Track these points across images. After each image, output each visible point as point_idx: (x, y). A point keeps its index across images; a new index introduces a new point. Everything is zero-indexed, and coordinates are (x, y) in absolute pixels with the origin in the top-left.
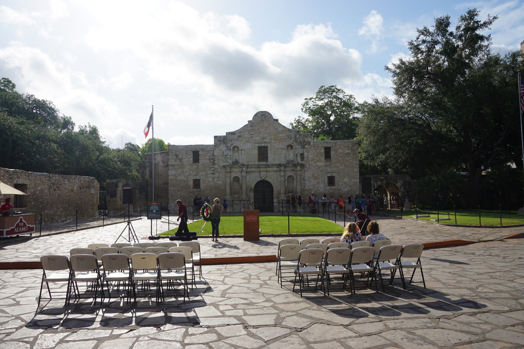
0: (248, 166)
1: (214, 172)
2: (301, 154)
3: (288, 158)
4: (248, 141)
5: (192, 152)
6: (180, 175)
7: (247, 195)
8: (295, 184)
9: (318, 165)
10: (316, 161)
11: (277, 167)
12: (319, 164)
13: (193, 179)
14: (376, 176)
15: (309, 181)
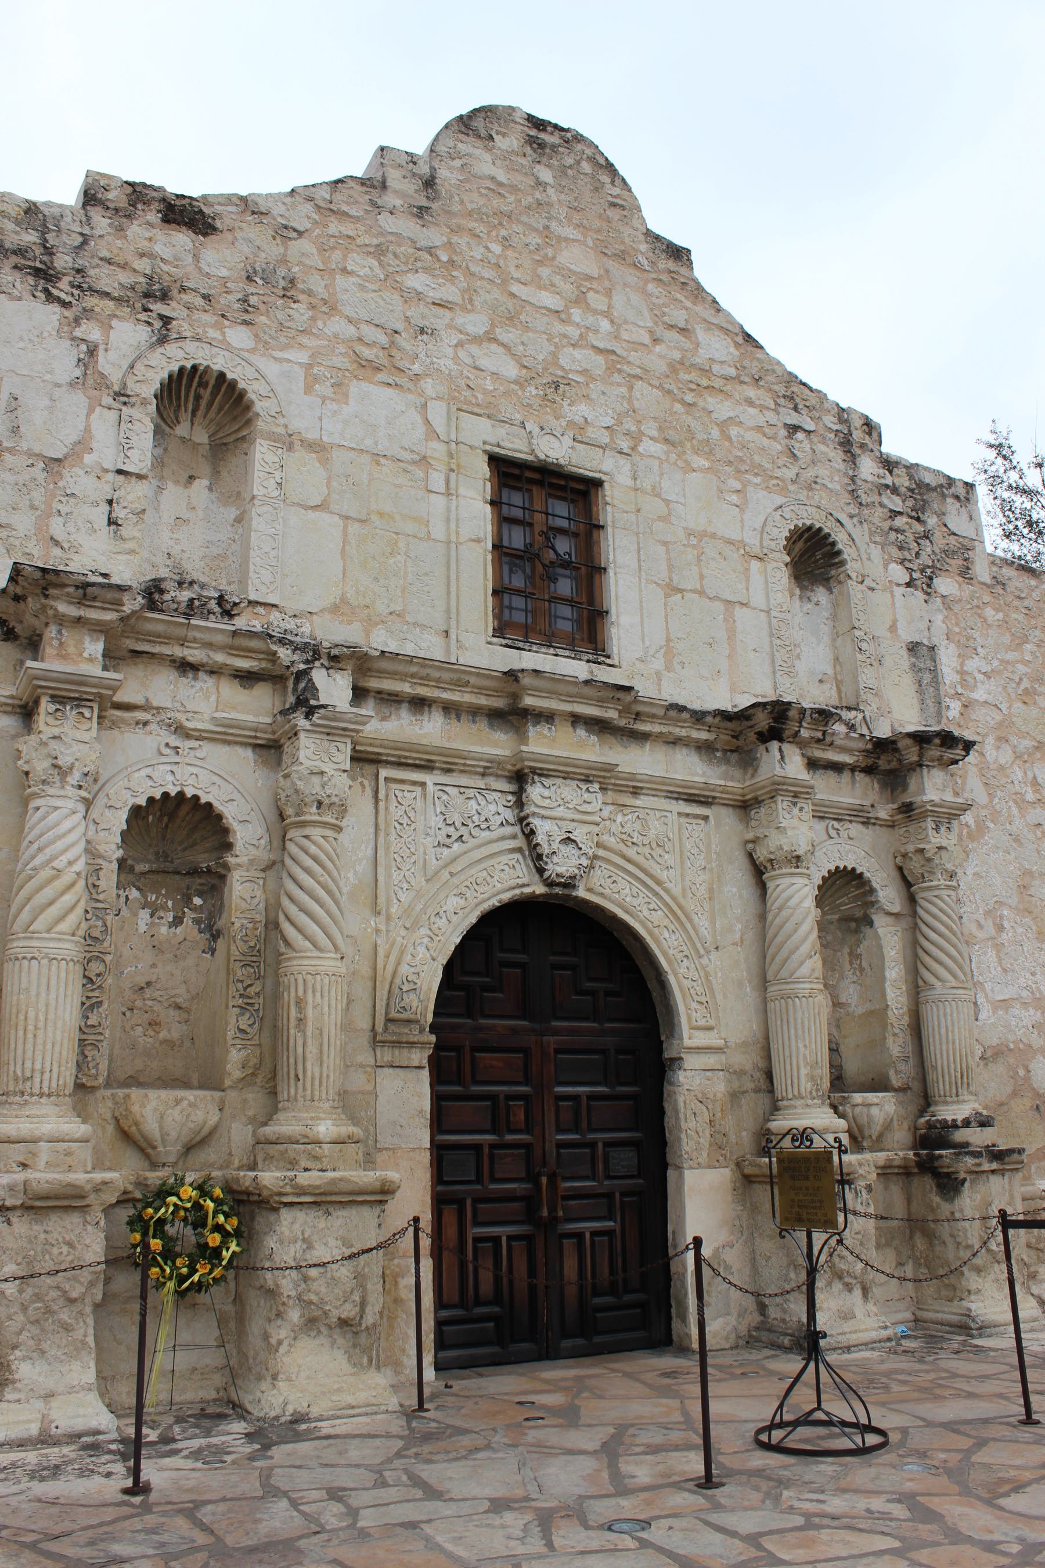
2: (913, 648)
4: (367, 353)
8: (894, 973)
11: (705, 748)
15: (999, 947)
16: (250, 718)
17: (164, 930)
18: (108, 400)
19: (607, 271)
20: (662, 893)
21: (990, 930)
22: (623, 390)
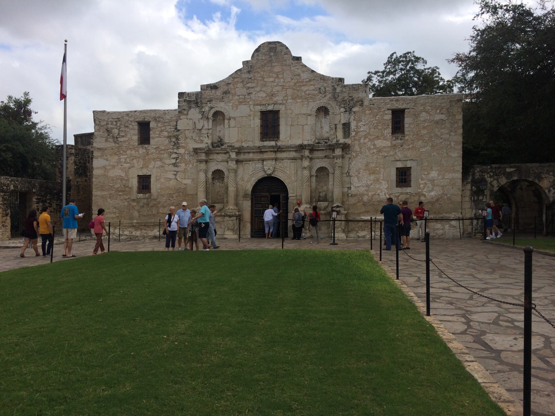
0: (240, 151)
1: (178, 161)
2: (344, 124)
3: (318, 134)
4: (241, 100)
5: (137, 123)
6: (114, 167)
7: (237, 204)
9: (377, 146)
10: (373, 137)
12: (380, 143)
13: (138, 176)
14: (497, 166)
16: (225, 159)
17: (221, 185)
18: (206, 119)
19: (283, 69)
20: (286, 174)
21: (357, 174)
22: (285, 92)
